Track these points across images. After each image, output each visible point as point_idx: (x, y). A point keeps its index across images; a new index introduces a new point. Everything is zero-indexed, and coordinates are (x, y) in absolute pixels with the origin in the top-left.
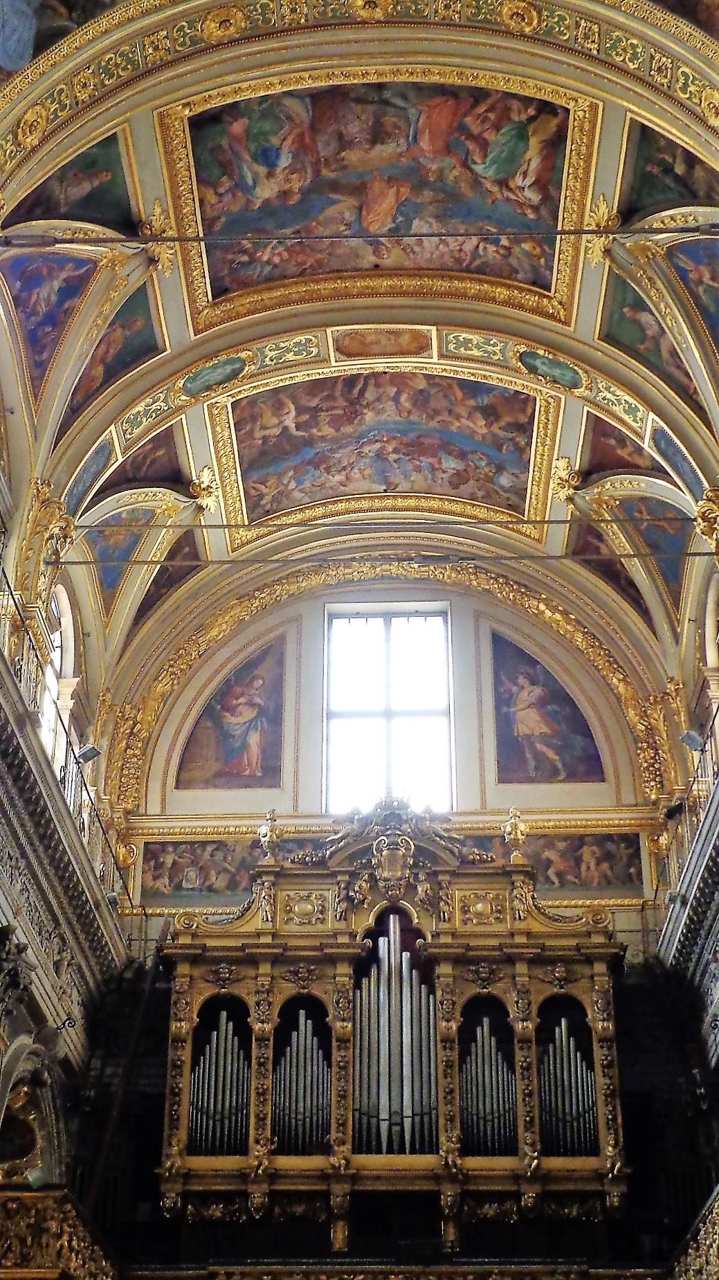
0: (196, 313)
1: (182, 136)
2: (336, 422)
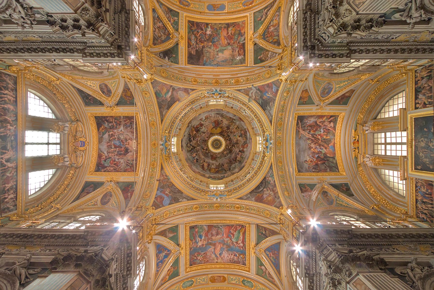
0: (186, 268)
1: (188, 228)
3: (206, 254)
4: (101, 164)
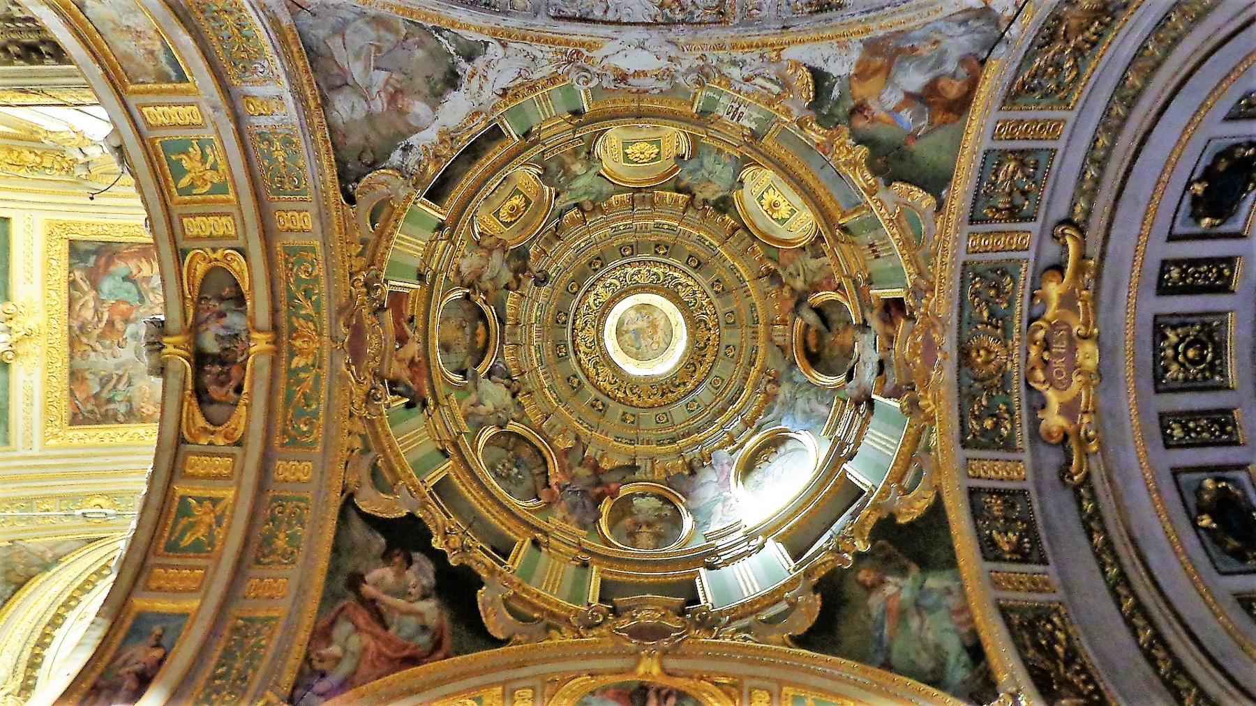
4: (110, 261)
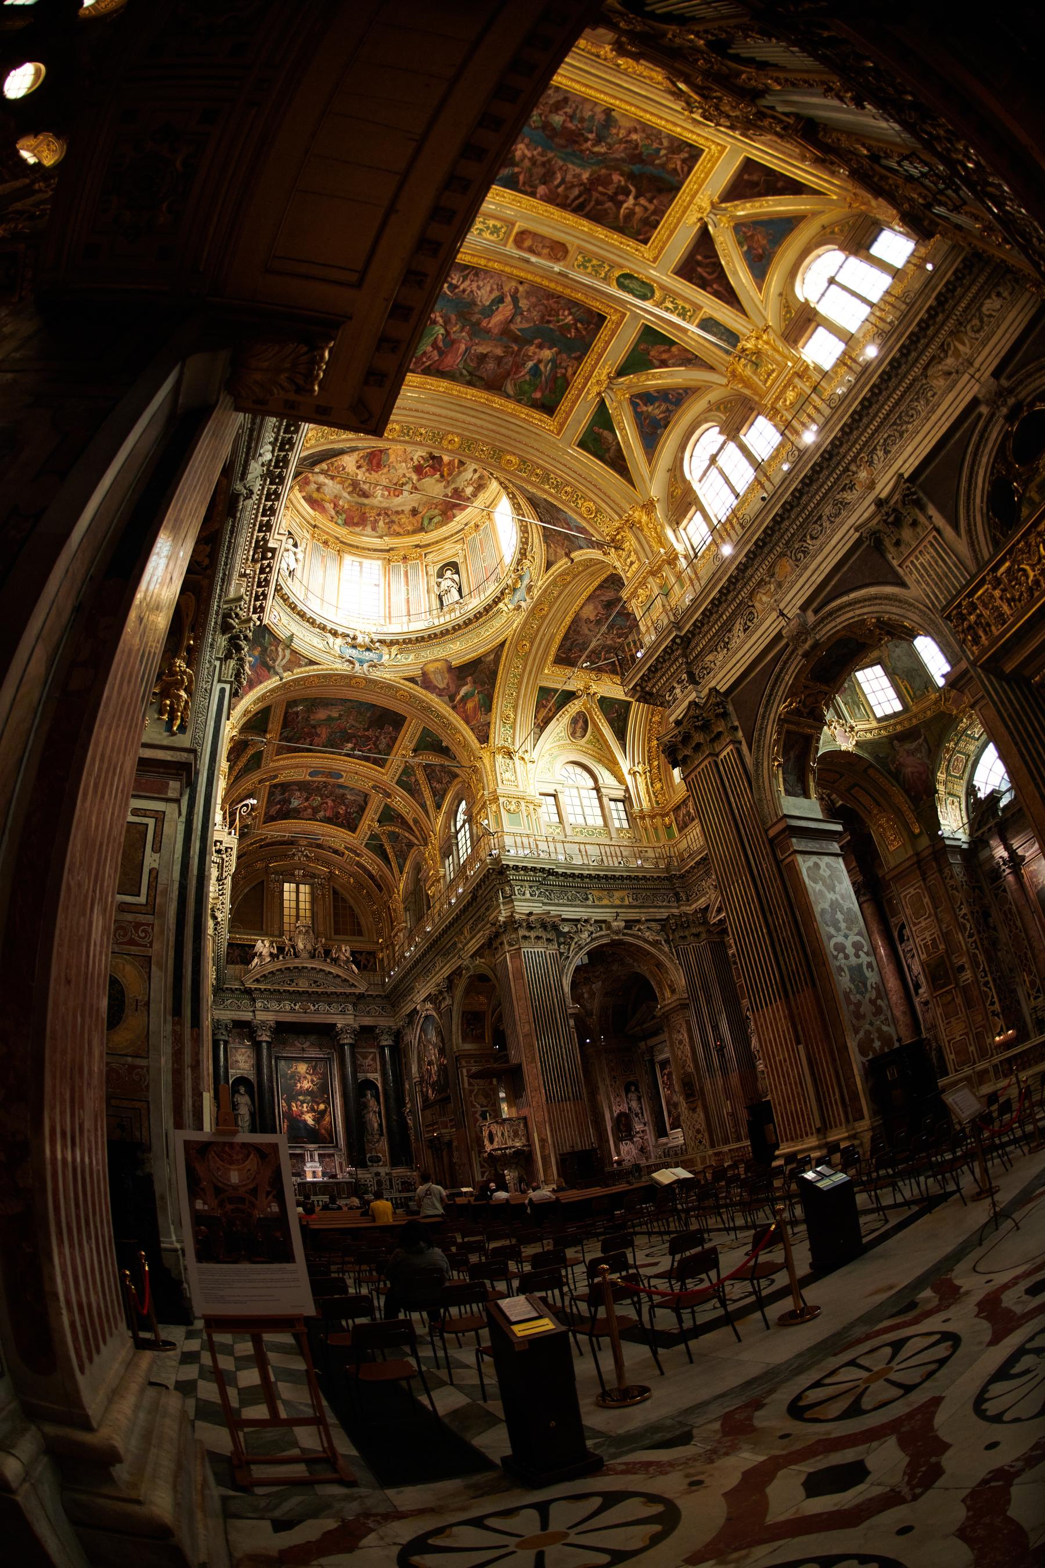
2: (606, 181)
3: (543, 317)
